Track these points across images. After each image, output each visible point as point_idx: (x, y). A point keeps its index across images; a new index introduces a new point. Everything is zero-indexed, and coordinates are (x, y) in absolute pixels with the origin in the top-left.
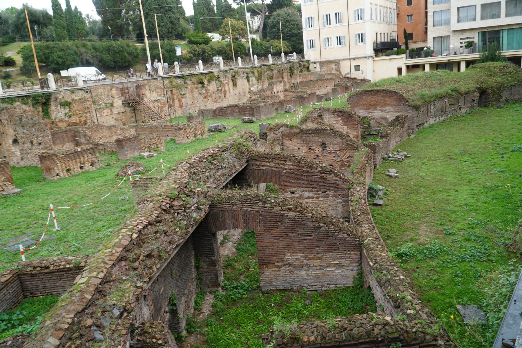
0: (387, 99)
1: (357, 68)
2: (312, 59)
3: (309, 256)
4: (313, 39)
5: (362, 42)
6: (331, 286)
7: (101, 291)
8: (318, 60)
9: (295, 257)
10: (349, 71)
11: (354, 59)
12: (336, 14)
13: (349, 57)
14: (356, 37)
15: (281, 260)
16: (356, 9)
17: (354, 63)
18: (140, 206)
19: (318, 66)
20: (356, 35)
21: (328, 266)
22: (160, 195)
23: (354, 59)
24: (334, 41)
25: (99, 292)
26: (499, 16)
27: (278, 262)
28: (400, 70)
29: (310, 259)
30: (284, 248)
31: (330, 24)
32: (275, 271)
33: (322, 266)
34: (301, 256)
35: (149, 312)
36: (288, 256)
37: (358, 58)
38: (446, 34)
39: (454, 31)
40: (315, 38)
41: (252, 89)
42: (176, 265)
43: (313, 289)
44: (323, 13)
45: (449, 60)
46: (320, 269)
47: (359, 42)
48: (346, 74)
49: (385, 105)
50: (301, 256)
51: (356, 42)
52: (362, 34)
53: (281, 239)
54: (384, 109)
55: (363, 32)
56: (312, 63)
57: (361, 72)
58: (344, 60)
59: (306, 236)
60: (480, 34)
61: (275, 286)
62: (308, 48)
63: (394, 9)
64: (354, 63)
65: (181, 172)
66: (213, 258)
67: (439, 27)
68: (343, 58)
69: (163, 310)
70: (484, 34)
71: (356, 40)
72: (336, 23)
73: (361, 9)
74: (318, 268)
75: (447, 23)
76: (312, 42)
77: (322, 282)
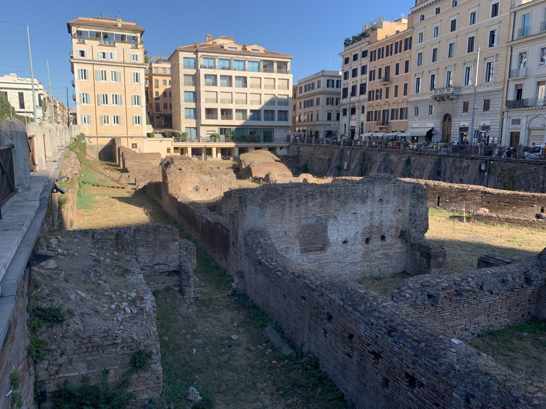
1: (134, 145)
8: (93, 135)
11: (132, 138)
12: (113, 95)
13: (126, 136)
17: (131, 141)
23: (132, 138)
24: (111, 120)
26: (216, 118)
28: (168, 150)
31: (107, 103)
44: (100, 92)
64: (131, 141)
70: (221, 129)
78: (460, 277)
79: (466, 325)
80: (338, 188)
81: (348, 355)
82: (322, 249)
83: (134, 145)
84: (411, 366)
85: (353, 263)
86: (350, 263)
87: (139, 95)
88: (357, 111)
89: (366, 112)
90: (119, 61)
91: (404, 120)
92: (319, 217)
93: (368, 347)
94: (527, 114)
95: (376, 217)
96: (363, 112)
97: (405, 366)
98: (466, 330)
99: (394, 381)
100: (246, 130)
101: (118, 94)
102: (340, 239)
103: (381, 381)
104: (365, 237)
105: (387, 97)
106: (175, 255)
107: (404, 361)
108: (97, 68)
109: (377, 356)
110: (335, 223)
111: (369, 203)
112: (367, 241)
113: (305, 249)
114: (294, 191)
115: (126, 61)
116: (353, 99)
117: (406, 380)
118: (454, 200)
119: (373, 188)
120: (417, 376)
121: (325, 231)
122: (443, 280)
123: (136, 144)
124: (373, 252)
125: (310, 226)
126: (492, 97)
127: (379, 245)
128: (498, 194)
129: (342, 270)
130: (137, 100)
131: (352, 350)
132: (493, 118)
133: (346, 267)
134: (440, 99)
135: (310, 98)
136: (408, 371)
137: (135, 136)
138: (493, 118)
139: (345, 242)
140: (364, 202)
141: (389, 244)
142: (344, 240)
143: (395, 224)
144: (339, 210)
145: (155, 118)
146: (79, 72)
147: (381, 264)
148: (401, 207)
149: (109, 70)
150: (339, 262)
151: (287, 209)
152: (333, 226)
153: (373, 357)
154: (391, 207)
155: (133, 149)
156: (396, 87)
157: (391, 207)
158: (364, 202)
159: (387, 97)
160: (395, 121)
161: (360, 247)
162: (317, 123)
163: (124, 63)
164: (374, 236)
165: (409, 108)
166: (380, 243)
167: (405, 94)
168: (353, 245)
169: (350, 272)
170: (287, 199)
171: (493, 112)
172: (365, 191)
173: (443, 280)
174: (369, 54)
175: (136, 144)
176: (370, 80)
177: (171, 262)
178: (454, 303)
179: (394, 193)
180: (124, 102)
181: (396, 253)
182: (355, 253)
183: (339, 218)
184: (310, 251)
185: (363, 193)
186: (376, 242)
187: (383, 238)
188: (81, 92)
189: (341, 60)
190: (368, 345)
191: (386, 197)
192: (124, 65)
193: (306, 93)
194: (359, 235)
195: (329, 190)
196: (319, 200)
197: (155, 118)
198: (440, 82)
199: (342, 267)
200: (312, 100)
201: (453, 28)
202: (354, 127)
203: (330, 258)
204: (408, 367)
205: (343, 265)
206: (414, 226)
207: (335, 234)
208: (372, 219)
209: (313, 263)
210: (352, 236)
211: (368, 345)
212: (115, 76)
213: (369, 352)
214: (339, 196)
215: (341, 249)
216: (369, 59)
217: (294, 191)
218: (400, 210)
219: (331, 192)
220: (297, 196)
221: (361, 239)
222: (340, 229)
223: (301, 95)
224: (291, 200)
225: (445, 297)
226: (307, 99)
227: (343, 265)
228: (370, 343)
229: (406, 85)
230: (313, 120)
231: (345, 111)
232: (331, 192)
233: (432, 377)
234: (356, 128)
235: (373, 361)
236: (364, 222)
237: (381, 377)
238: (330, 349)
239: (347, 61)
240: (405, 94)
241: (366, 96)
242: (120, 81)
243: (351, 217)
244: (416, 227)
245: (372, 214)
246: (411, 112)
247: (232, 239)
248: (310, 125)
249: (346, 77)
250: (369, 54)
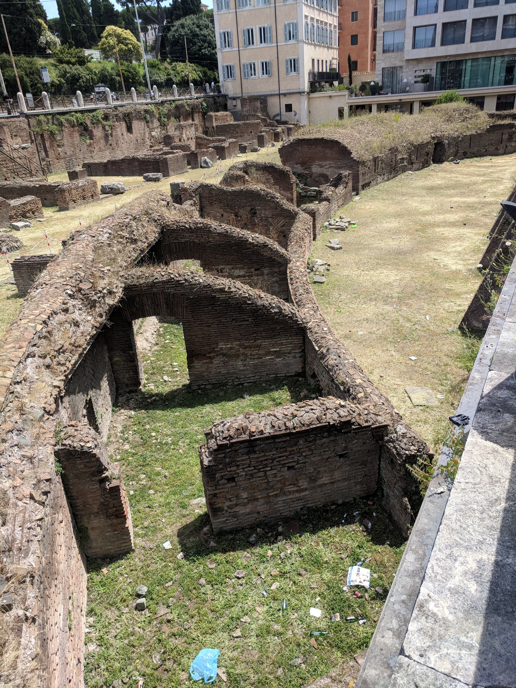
0: (328, 151)
1: (289, 108)
2: (231, 94)
3: (246, 344)
4: (232, 64)
5: (295, 71)
6: (271, 376)
7: (13, 393)
9: (230, 346)
10: (278, 112)
11: (285, 95)
13: (278, 92)
14: (287, 64)
15: (213, 351)
16: (286, 23)
17: (285, 101)
18: (38, 291)
19: (239, 103)
20: (287, 61)
21: (268, 353)
22: (62, 277)
25: (11, 393)
27: (210, 353)
29: (245, 348)
30: (216, 337)
31: (253, 43)
32: (206, 363)
33: (259, 354)
34: (237, 345)
35: (67, 415)
36: (222, 345)
38: (398, 64)
39: (408, 60)
40: (233, 62)
41: (153, 134)
42: (89, 362)
43: (251, 381)
44: (244, 26)
45: (400, 100)
46: (259, 358)
47: (291, 71)
48: (275, 116)
49: (325, 159)
50: (237, 345)
51: (287, 72)
52: (294, 60)
53: (212, 326)
54: (324, 163)
55: (296, 57)
56: (231, 98)
57: (293, 113)
58: (271, 95)
59: (242, 321)
60: (439, 65)
61: (208, 380)
62: (224, 78)
63: (335, 26)
64: (285, 101)
65: (83, 247)
66: (131, 352)
67: (390, 54)
68: (270, 93)
69: (81, 414)
71: (287, 68)
72: (261, 42)
73: (293, 24)
74: (256, 357)
75: (399, 48)
76: (229, 70)
77: (261, 372)
100: (493, 59)
101: (266, 25)
137: (289, 91)
188: (221, 31)
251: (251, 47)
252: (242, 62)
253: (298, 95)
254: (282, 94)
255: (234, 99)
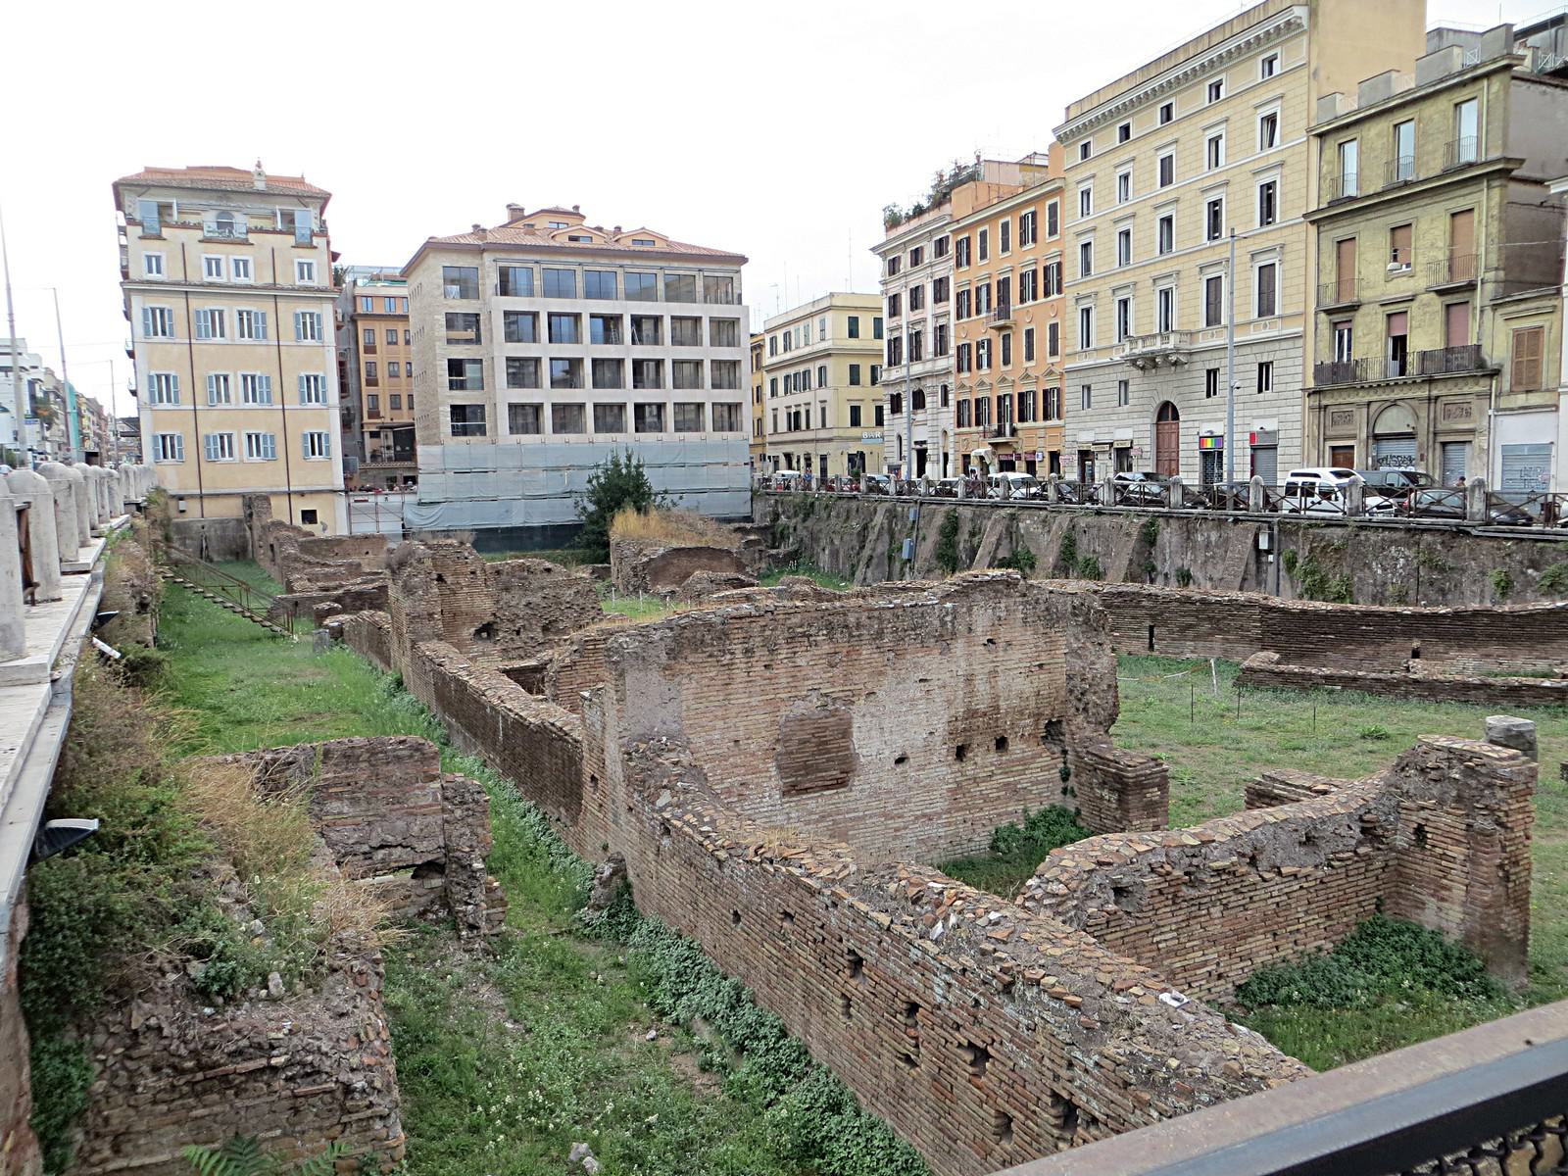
1: (309, 516)
11: (302, 494)
17: (301, 505)
37: (312, 492)
44: (205, 370)
47: (313, 453)
51: (306, 454)
56: (173, 497)
62: (157, 456)
78: (1194, 835)
79: (1218, 964)
80: (876, 614)
81: (908, 1059)
82: (841, 783)
83: (309, 516)
84: (1064, 1073)
85: (924, 816)
86: (917, 818)
87: (321, 374)
88: (928, 400)
89: (952, 403)
90: (259, 283)
91: (1054, 422)
92: (826, 695)
93: (957, 1034)
94: (1367, 399)
95: (982, 687)
96: (945, 403)
97: (1050, 1074)
98: (1220, 976)
99: (1027, 1118)
101: (258, 374)
102: (887, 753)
103: (993, 1121)
104: (955, 745)
105: (1006, 362)
106: (430, 819)
107: (1046, 1062)
108: (196, 303)
109: (981, 1055)
110: (873, 710)
111: (959, 647)
112: (961, 753)
113: (793, 786)
114: (756, 628)
115: (280, 281)
116: (917, 369)
117: (1053, 1112)
118: (1191, 633)
119: (970, 609)
120: (1081, 1099)
121: (846, 734)
122: (1153, 845)
123: (314, 512)
124: (975, 780)
125: (801, 720)
126: (1279, 355)
127: (992, 764)
128: (1304, 612)
129: (895, 838)
130: (311, 386)
131: (917, 1046)
132: (1283, 411)
133: (905, 828)
134: (1149, 363)
135: (801, 369)
136: (1057, 1087)
138: (1283, 411)
139: (900, 761)
140: (946, 650)
141: (1019, 760)
142: (897, 756)
143: (1032, 703)
144: (881, 673)
145: (367, 436)
146: (145, 318)
147: (999, 815)
148: (1044, 659)
149: (231, 309)
150: (887, 816)
151: (740, 675)
152: (868, 718)
153: (969, 1057)
154: (1016, 659)
155: (308, 527)
156: (1029, 333)
157: (1016, 659)
158: (946, 650)
159: (1006, 362)
160: (1030, 424)
161: (942, 771)
162: (823, 434)
163: (274, 286)
164: (978, 739)
165: (1066, 390)
166: (994, 756)
167: (1054, 352)
168: (921, 768)
169: (918, 841)
170: (738, 649)
171: (1283, 395)
172: (948, 618)
173: (1153, 845)
174: (951, 248)
175: (314, 512)
176: (959, 316)
177: (421, 838)
178: (1184, 905)
179: (1025, 621)
180: (276, 396)
181: (1038, 783)
182: (928, 789)
183: (881, 694)
184: (806, 790)
185: (943, 624)
186: (983, 758)
187: (1001, 744)
189: (879, 266)
190: (958, 1027)
191: (1003, 634)
192: (274, 292)
193: (788, 356)
194: (938, 739)
195: (852, 620)
196: (826, 648)
197: (367, 436)
198: (1145, 317)
199: (896, 830)
200: (807, 373)
201: (1166, 179)
202: (925, 442)
203: (861, 807)
204: (1057, 1078)
205: (899, 823)
206: (1081, 706)
207: (870, 742)
208: (971, 693)
209: (817, 821)
210: (920, 743)
211: (958, 1027)
212: (248, 324)
213: (960, 1045)
214: (880, 634)
215: (890, 779)
216: (953, 262)
217: (756, 628)
218: (1041, 666)
219: (858, 626)
220: (765, 639)
221: (943, 751)
222: (886, 725)
223: (775, 359)
224: (748, 652)
225: (1161, 892)
226: (792, 371)
227: (899, 823)
228: (960, 1022)
229: (1054, 328)
230: (812, 426)
231: (896, 403)
232: (858, 626)
233: (1116, 1097)
234: (929, 446)
235: (971, 1069)
236: (950, 703)
237: (993, 1112)
238: (862, 1047)
239: (893, 266)
240: (1054, 352)
241: (949, 362)
242: (265, 336)
243: (916, 691)
244: (1085, 710)
245: (969, 679)
246: (1071, 398)
247: (588, 769)
248: (803, 441)
249: (894, 311)
250: (951, 248)
251: (224, 405)
252: (202, 432)
253: (330, 496)
254: (296, 492)
255: (181, 498)
